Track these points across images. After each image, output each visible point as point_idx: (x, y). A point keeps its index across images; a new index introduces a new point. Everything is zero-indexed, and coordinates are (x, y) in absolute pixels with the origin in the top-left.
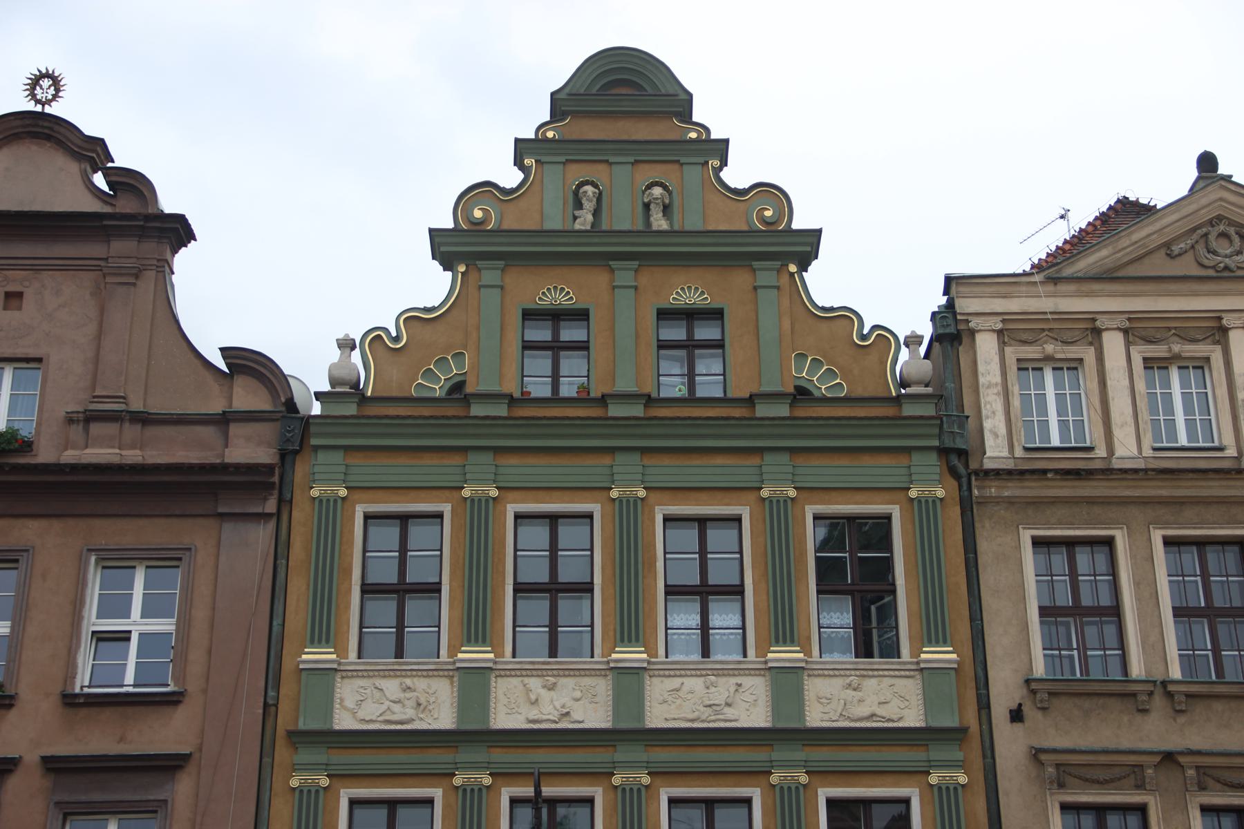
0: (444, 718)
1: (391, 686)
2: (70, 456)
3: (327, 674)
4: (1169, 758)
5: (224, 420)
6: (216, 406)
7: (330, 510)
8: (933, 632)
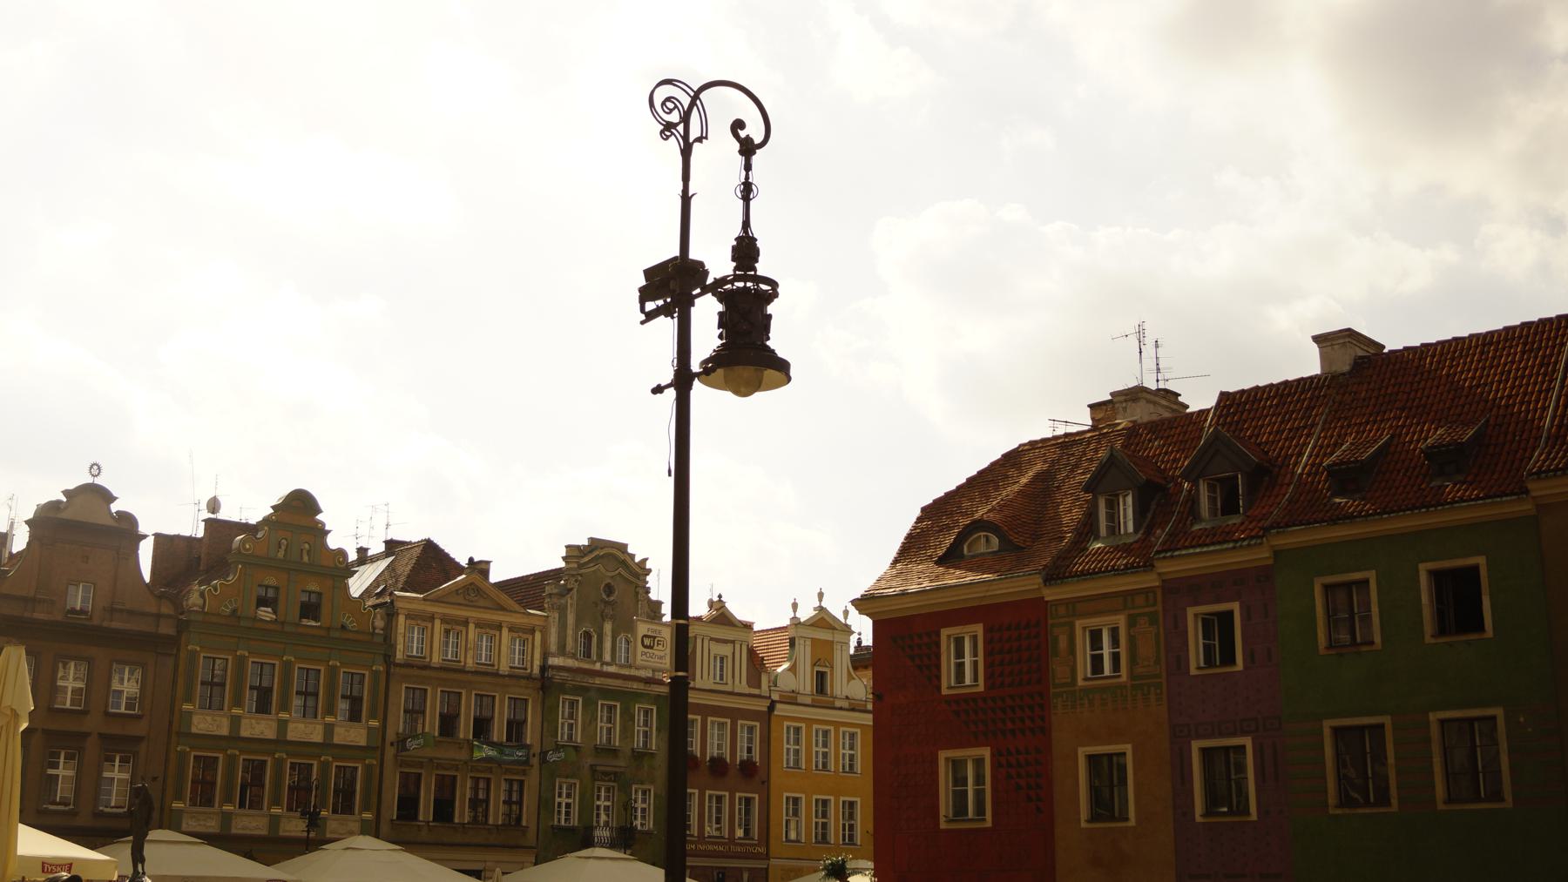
0: (225, 731)
1: (209, 718)
2: (105, 624)
3: (190, 713)
4: (431, 760)
5: (158, 616)
6: (154, 610)
7: (194, 654)
8: (372, 716)
